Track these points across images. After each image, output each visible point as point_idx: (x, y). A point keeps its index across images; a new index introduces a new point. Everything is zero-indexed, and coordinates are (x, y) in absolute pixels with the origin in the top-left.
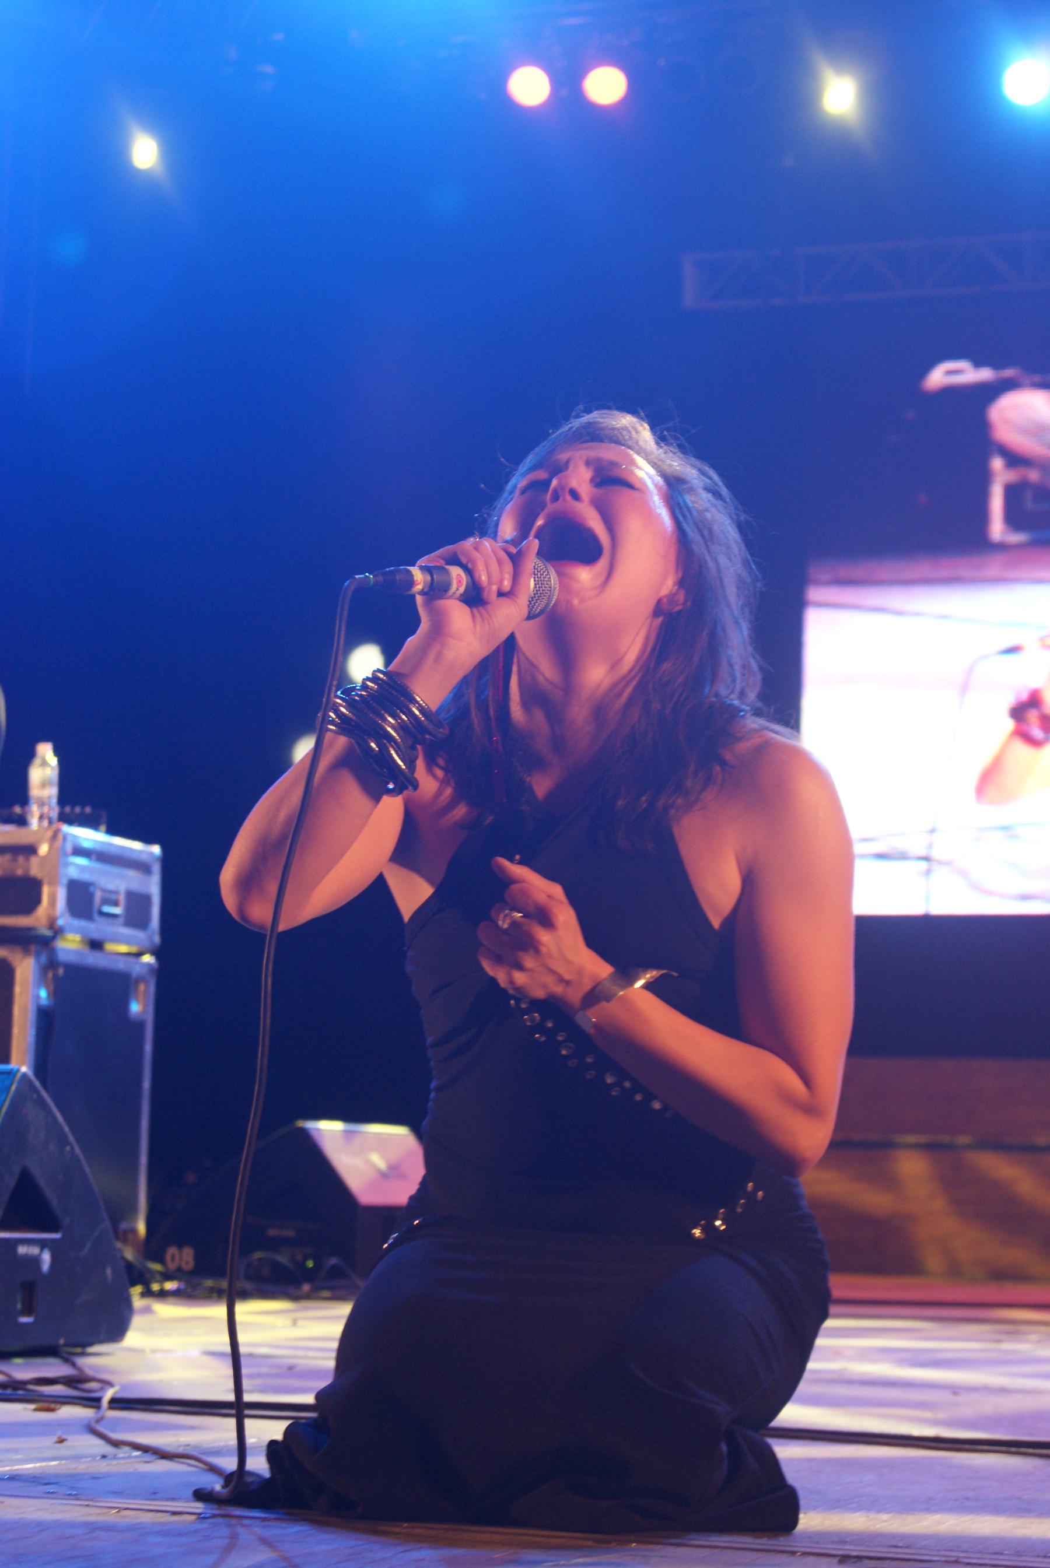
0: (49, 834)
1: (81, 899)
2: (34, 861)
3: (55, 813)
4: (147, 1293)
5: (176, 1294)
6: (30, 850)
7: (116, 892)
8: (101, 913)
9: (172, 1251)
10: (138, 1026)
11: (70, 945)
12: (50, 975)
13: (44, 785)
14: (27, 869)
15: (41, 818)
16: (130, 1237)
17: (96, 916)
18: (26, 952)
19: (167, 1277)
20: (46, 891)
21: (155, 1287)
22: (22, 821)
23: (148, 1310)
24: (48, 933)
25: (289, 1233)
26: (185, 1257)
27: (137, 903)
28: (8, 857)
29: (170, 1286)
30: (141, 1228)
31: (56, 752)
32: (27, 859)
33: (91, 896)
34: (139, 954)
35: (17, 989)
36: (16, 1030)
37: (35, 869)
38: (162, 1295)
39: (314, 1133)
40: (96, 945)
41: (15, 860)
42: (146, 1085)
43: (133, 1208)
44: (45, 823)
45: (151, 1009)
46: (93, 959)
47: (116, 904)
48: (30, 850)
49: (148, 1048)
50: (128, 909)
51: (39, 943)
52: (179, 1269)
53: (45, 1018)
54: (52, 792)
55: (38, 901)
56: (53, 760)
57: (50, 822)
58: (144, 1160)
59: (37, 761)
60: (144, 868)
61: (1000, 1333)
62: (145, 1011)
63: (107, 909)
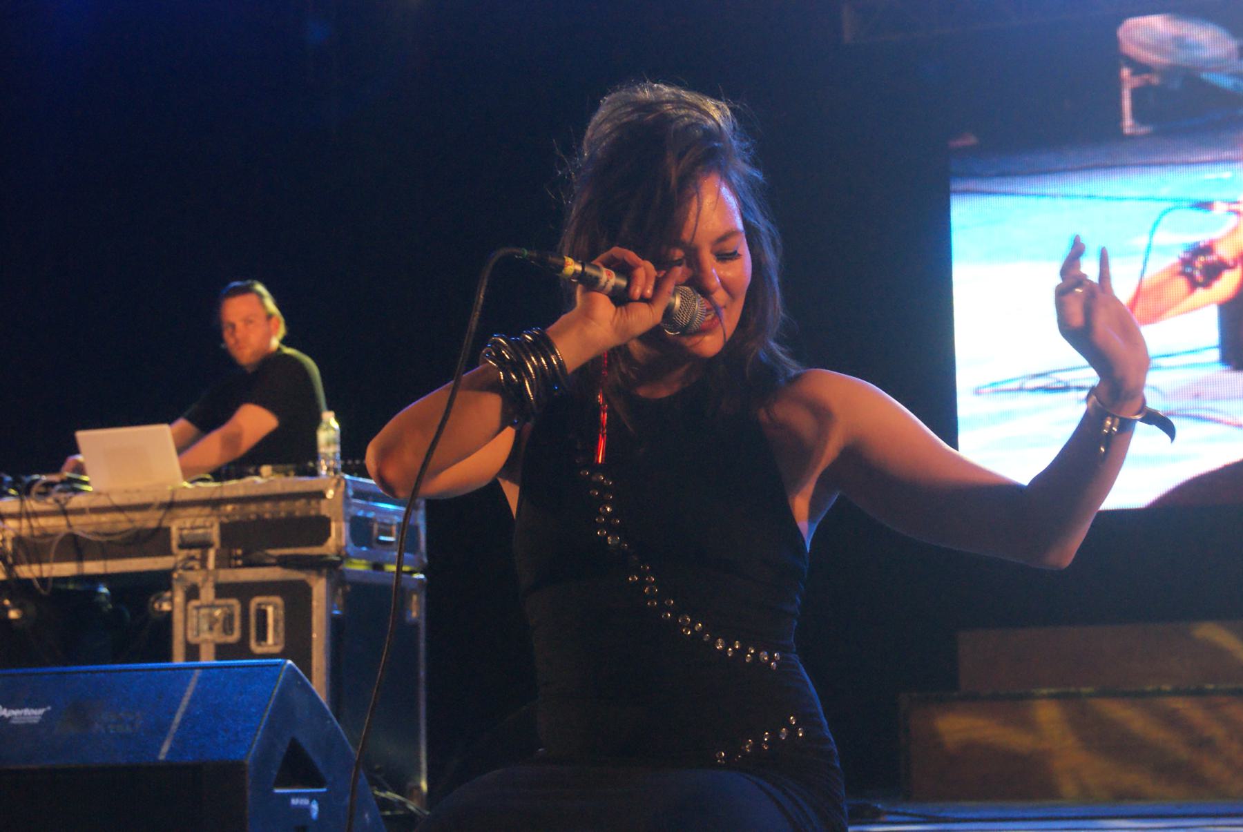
0: (334, 481)
1: (361, 531)
2: (323, 503)
3: (339, 466)
6: (321, 495)
7: (391, 525)
10: (415, 626)
11: (359, 566)
12: (340, 591)
13: (328, 444)
14: (319, 509)
15: (329, 469)
16: (416, 792)
17: (375, 545)
18: (320, 575)
20: (333, 525)
22: (314, 473)
24: (337, 559)
30: (424, 785)
31: (337, 418)
32: (318, 503)
33: (371, 528)
35: (315, 603)
36: (314, 636)
37: (325, 509)
40: (378, 567)
41: (309, 504)
42: (422, 674)
43: (419, 771)
44: (332, 474)
45: (423, 615)
46: (376, 578)
47: (389, 534)
49: (422, 645)
53: (337, 627)
54: (335, 449)
55: (328, 534)
56: (335, 424)
57: (336, 472)
58: (423, 732)
59: (324, 426)
62: (419, 618)
63: (382, 538)
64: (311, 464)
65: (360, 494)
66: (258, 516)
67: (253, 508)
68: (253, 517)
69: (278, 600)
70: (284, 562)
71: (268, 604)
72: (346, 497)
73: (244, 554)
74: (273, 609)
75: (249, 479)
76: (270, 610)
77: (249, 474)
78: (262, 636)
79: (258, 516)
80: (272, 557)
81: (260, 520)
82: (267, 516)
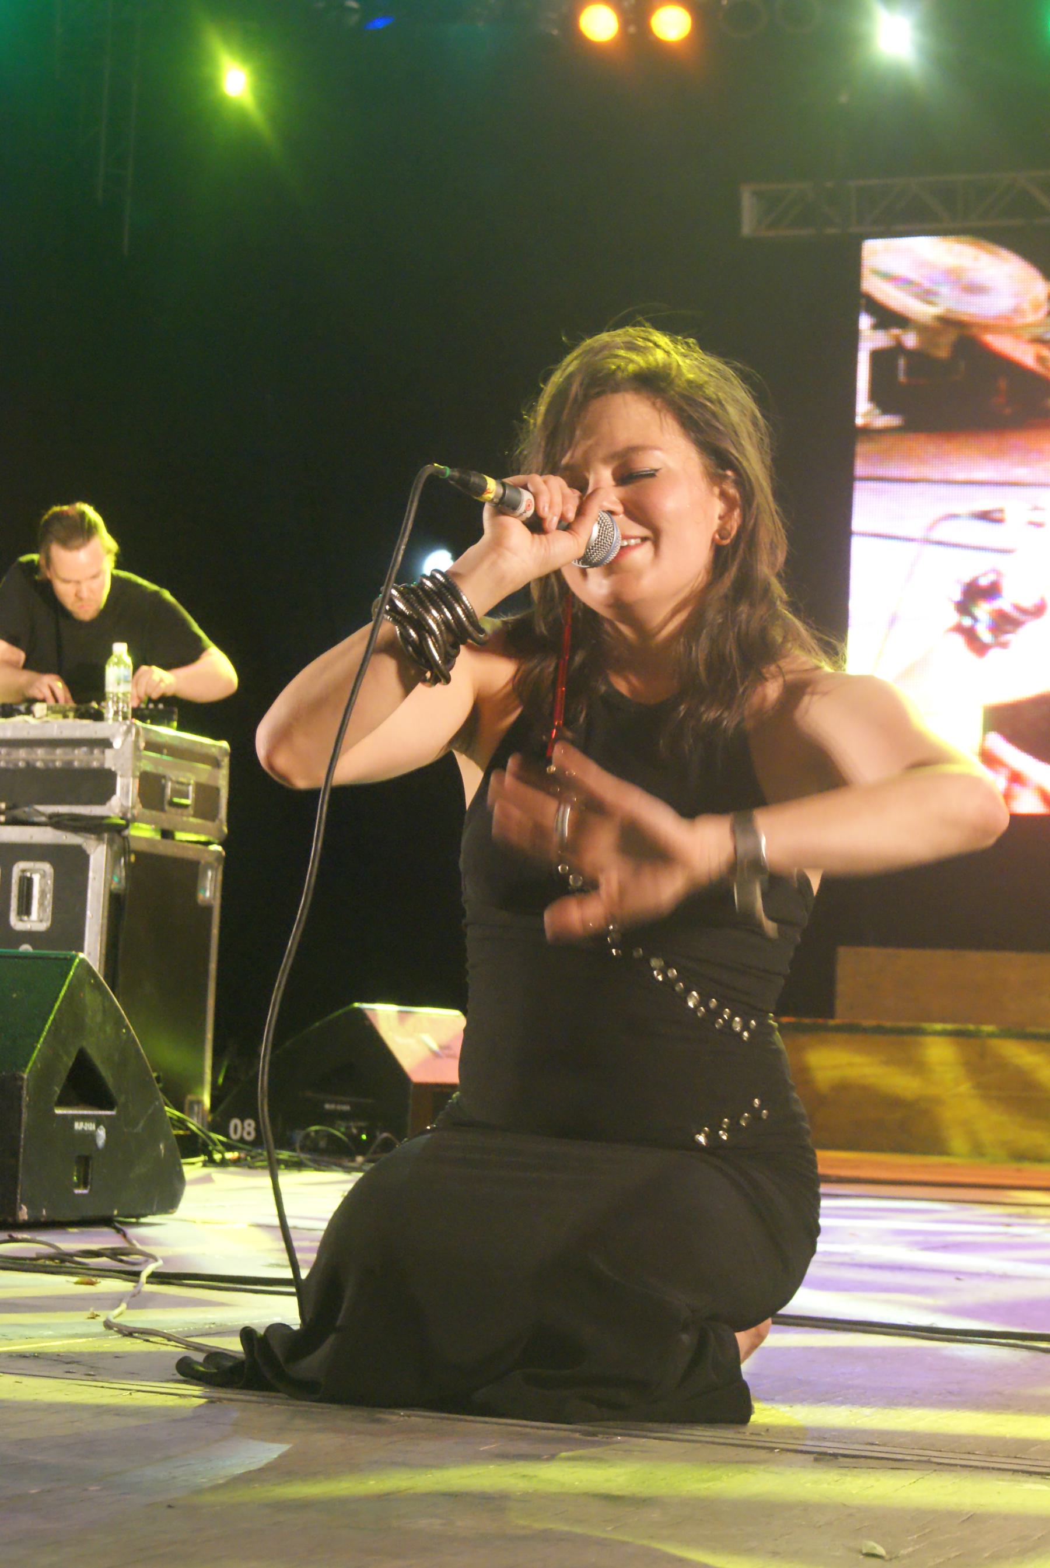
0: (125, 728)
1: (152, 791)
4: (211, 1162)
5: (236, 1163)
6: (105, 744)
8: (172, 804)
9: (235, 1121)
10: (208, 909)
11: (143, 832)
15: (116, 713)
16: (196, 1108)
17: (167, 807)
18: (100, 839)
19: (229, 1148)
20: (119, 780)
21: (217, 1157)
23: (208, 1179)
24: (123, 822)
25: (346, 1108)
26: (244, 1128)
27: (206, 794)
28: (84, 749)
29: (230, 1155)
33: (163, 788)
34: (207, 843)
35: (91, 874)
36: (89, 913)
37: (110, 760)
38: (224, 1163)
39: (369, 1013)
40: (167, 834)
41: (92, 753)
42: (213, 966)
43: (201, 1082)
44: (120, 718)
45: (218, 895)
46: (166, 848)
47: (187, 797)
48: (105, 744)
49: (215, 931)
50: (197, 800)
51: (112, 831)
52: (242, 1140)
53: (116, 902)
57: (125, 718)
58: (209, 1035)
59: (113, 659)
60: (216, 764)
61: (1010, 1216)
63: (176, 800)
64: (95, 705)
65: (152, 746)
66: (28, 763)
67: (22, 753)
68: (21, 764)
69: (47, 867)
70: (57, 822)
71: (33, 871)
72: (136, 747)
73: (8, 808)
74: (41, 876)
75: (18, 719)
76: (36, 878)
77: (20, 713)
78: (25, 909)
79: (28, 763)
80: (43, 814)
81: (30, 767)
82: (39, 764)
